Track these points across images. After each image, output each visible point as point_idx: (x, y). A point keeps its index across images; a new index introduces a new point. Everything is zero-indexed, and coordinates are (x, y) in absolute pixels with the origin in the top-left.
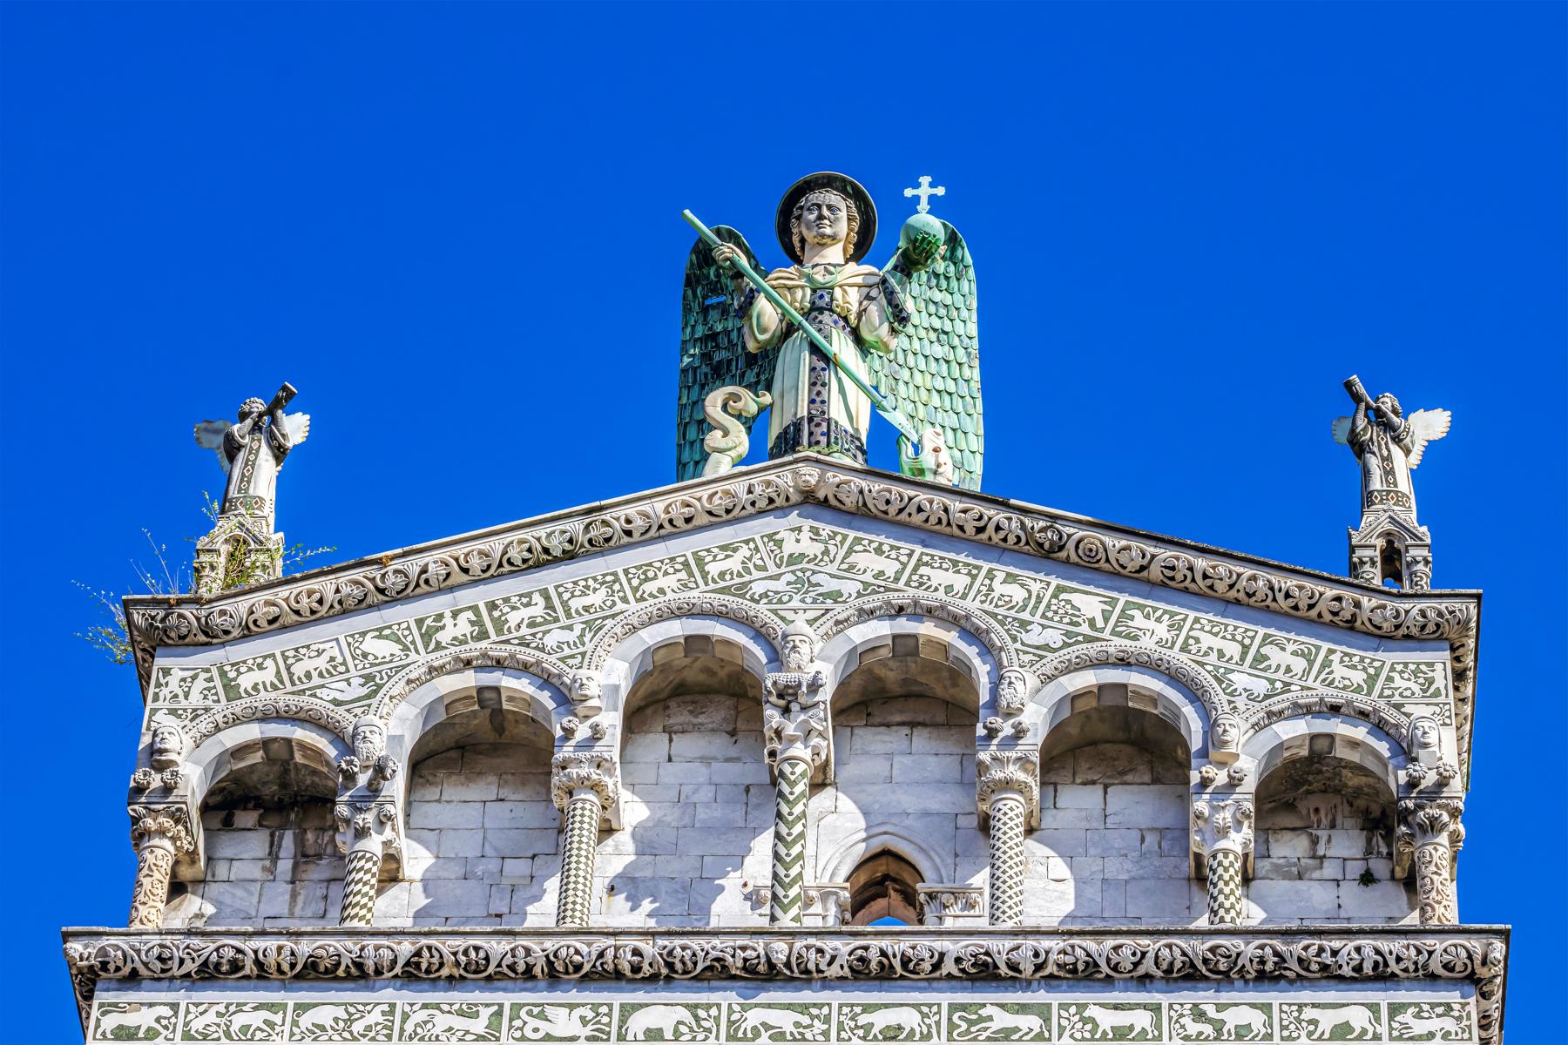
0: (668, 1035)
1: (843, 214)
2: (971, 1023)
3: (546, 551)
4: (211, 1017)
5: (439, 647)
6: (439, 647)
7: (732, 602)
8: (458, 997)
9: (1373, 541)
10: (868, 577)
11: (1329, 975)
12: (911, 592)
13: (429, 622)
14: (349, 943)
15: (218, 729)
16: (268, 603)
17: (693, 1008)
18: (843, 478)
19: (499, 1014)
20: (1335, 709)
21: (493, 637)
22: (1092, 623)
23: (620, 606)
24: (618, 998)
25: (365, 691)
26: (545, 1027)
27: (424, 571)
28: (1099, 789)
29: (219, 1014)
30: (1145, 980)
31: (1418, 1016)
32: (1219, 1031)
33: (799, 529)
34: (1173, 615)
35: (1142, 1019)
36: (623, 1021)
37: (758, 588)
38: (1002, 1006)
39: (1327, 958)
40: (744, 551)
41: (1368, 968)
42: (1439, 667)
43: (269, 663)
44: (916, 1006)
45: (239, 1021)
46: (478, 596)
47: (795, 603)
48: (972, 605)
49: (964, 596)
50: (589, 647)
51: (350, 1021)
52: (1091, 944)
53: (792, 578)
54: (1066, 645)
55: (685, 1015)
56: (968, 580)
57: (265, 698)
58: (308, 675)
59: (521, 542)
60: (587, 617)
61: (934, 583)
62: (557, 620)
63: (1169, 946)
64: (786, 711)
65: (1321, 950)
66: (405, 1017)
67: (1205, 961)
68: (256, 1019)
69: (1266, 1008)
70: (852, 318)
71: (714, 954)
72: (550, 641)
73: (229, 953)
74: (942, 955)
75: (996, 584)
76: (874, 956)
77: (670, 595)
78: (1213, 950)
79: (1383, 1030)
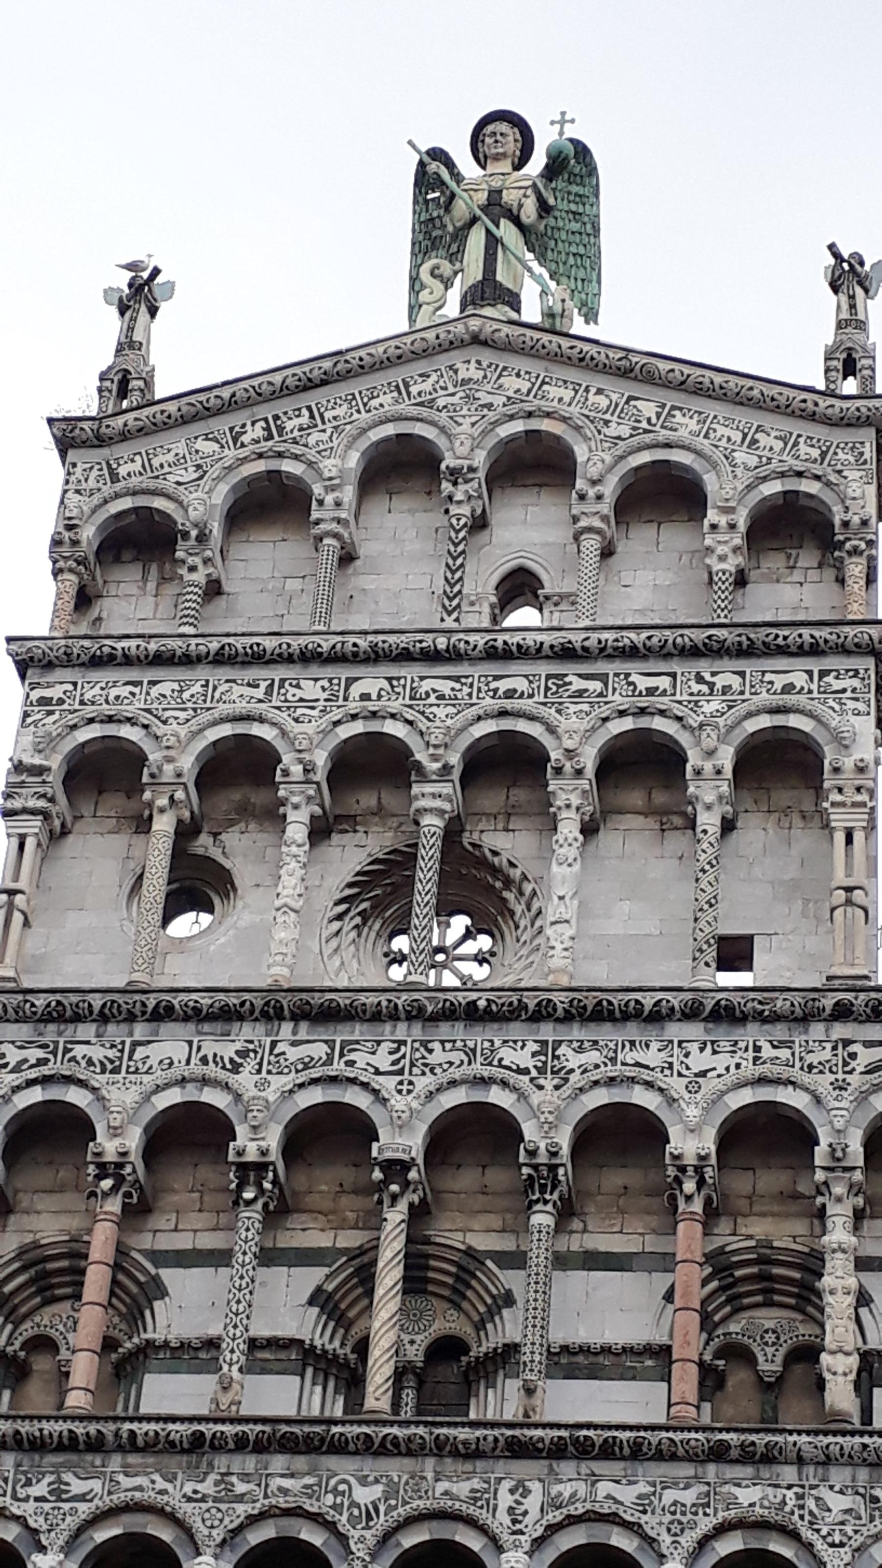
0: (374, 697)
1: (511, 138)
2: (559, 686)
3: (310, 380)
4: (97, 690)
5: (243, 445)
6: (243, 445)
7: (424, 412)
9: (837, 355)
10: (510, 393)
11: (783, 651)
12: (536, 402)
13: (237, 429)
14: (179, 642)
15: (106, 502)
16: (136, 419)
17: (389, 679)
18: (495, 327)
19: (272, 685)
20: (800, 474)
21: (277, 438)
22: (649, 420)
23: (356, 416)
24: (344, 672)
25: (196, 475)
26: (299, 694)
27: (233, 395)
28: (655, 525)
29: (102, 689)
30: (668, 656)
31: (837, 678)
32: (712, 690)
33: (469, 362)
34: (700, 413)
35: (664, 683)
36: (347, 689)
37: (441, 402)
38: (580, 676)
39: (780, 640)
40: (434, 377)
41: (806, 647)
42: (868, 445)
43: (138, 458)
44: (526, 676)
45: (113, 692)
46: (266, 411)
47: (464, 412)
48: (574, 410)
49: (570, 405)
50: (335, 443)
51: (181, 691)
52: (632, 635)
53: (462, 394)
54: (632, 436)
55: (385, 684)
56: (572, 393)
57: (135, 481)
58: (162, 466)
59: (294, 375)
60: (335, 423)
61: (551, 396)
62: (316, 426)
63: (682, 636)
64: (455, 484)
65: (777, 636)
66: (215, 688)
67: (705, 644)
68: (125, 691)
69: (742, 674)
70: (515, 212)
71: (402, 645)
72: (311, 440)
73: (106, 650)
74: (542, 644)
75: (590, 396)
76: (499, 644)
77: (387, 408)
78: (709, 637)
79: (814, 687)
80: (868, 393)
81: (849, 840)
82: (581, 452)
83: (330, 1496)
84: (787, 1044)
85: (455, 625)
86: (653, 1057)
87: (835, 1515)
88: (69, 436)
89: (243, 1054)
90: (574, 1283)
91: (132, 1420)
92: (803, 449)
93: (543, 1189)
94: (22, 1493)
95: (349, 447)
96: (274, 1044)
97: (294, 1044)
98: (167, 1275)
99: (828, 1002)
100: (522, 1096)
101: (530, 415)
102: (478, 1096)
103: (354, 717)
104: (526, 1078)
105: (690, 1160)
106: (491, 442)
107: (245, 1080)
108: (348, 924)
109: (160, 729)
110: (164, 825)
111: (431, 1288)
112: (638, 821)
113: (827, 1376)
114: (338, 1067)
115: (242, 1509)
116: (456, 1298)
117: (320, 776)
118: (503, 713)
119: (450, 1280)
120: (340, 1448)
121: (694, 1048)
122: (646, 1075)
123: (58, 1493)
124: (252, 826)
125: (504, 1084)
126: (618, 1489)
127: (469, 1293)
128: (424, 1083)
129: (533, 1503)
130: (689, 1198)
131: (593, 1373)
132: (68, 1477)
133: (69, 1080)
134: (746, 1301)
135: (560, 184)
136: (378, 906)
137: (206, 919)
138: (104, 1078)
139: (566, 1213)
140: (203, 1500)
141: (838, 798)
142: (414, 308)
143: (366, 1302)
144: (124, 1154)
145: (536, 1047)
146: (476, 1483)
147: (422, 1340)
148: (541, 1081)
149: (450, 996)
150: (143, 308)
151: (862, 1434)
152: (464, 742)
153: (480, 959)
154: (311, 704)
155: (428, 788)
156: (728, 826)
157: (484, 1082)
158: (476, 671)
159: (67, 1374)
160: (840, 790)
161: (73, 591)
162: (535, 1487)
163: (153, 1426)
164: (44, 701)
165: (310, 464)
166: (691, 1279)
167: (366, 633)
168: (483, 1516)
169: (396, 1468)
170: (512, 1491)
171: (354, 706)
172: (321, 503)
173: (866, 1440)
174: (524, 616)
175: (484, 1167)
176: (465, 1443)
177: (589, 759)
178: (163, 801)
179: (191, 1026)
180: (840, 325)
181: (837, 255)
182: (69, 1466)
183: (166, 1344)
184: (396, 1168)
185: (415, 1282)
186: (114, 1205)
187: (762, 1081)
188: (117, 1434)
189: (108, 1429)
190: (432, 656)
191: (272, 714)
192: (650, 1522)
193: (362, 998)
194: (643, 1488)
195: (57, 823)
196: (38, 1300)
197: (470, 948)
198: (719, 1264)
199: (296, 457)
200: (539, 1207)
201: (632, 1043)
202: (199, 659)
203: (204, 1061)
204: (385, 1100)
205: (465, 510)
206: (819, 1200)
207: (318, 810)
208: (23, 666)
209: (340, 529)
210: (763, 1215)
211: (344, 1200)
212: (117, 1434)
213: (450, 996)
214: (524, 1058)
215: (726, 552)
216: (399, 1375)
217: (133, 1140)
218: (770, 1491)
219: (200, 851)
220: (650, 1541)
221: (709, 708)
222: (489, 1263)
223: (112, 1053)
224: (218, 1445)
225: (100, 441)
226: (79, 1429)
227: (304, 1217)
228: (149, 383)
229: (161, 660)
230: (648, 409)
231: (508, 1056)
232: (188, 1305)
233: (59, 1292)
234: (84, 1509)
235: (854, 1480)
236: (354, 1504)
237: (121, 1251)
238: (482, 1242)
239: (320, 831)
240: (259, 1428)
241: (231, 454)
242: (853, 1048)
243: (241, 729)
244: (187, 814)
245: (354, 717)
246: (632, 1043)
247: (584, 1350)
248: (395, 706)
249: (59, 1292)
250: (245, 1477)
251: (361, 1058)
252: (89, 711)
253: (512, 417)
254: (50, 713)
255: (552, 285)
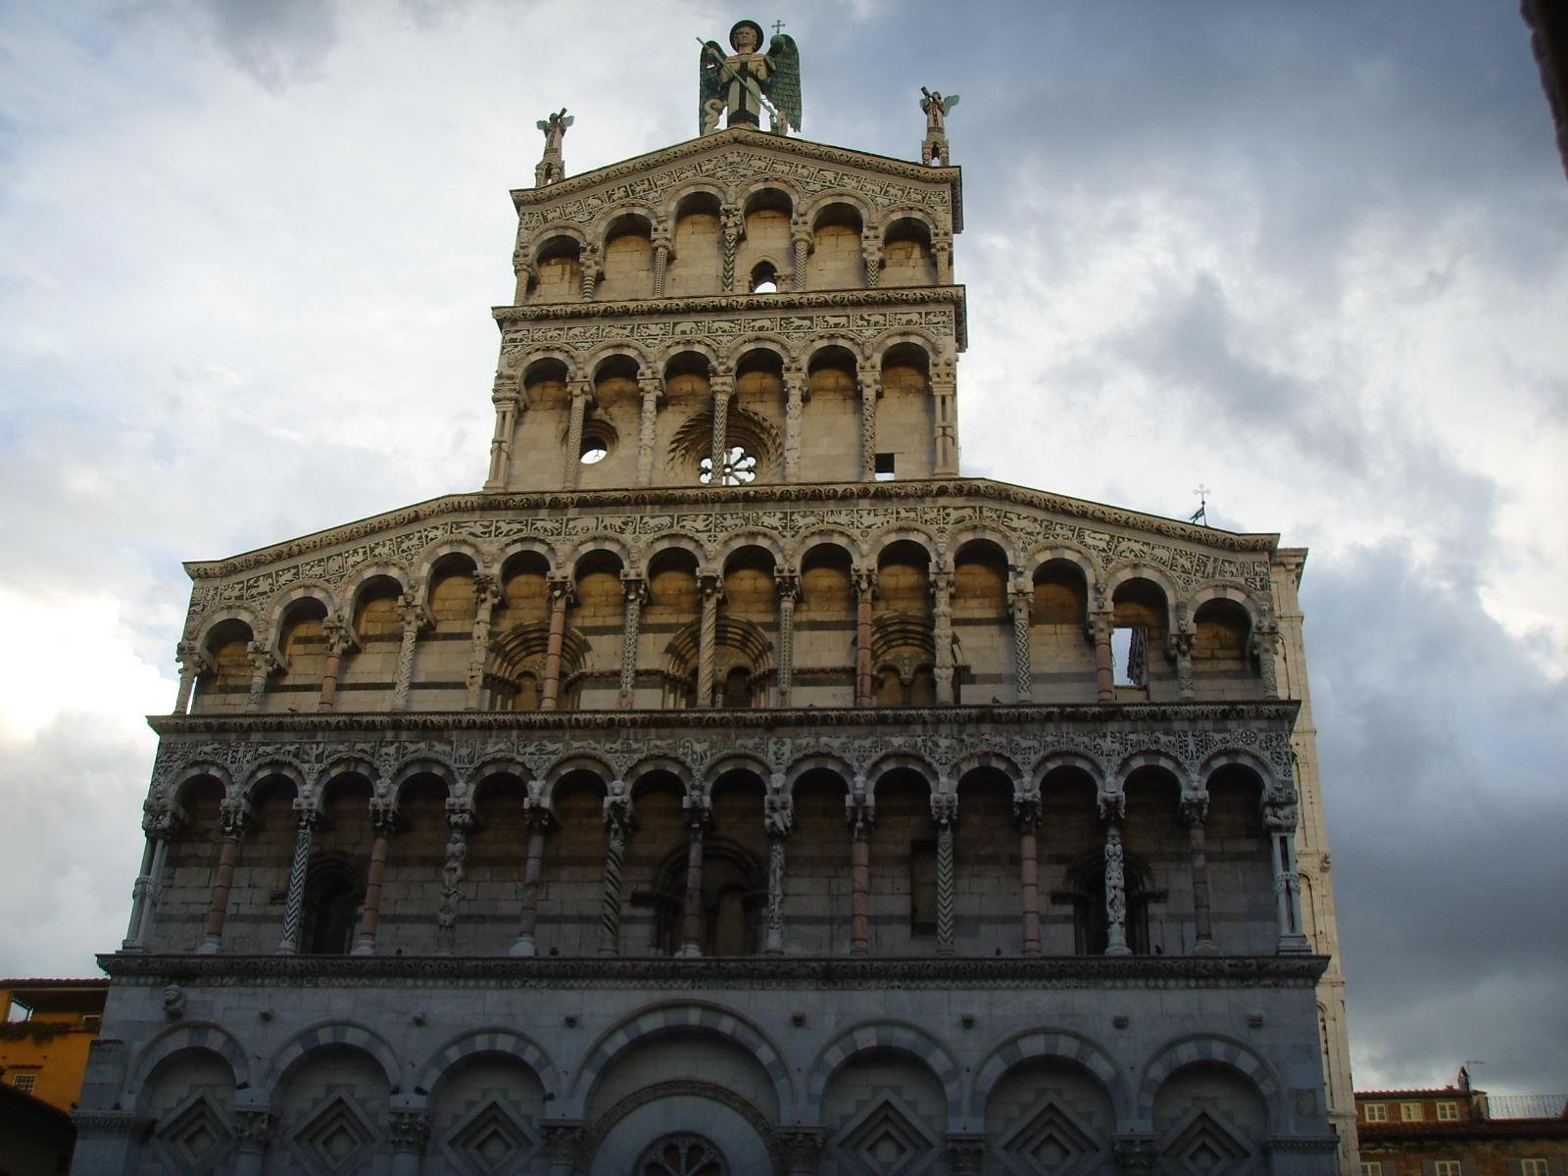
1: (751, 36)
4: (540, 334)
8: (620, 324)
11: (906, 302)
24: (672, 320)
26: (648, 332)
30: (846, 305)
35: (843, 321)
37: (719, 175)
45: (550, 334)
46: (626, 182)
48: (790, 177)
55: (694, 325)
64: (728, 217)
68: (555, 333)
69: (885, 315)
72: (650, 197)
80: (944, 165)
81: (943, 402)
82: (795, 199)
83: (681, 750)
84: (914, 510)
85: (730, 293)
86: (843, 519)
87: (942, 749)
88: (522, 200)
89: (626, 523)
90: (804, 637)
91: (577, 713)
92: (913, 195)
93: (787, 589)
94: (522, 751)
95: (670, 200)
96: (642, 518)
97: (652, 517)
98: (592, 640)
99: (935, 487)
100: (775, 542)
101: (767, 179)
102: (751, 542)
103: (678, 343)
104: (776, 532)
105: (864, 572)
106: (747, 195)
107: (627, 537)
108: (678, 454)
109: (574, 353)
110: (579, 404)
111: (729, 642)
112: (831, 396)
113: (938, 680)
114: (676, 529)
115: (637, 756)
116: (743, 645)
117: (661, 375)
118: (758, 339)
119: (739, 638)
120: (684, 724)
121: (865, 513)
122: (840, 528)
123: (541, 750)
124: (625, 403)
125: (765, 535)
126: (831, 741)
127: (750, 644)
128: (722, 536)
129: (787, 749)
130: (863, 591)
131: (816, 683)
132: (545, 742)
133: (535, 540)
134: (894, 643)
135: (779, 58)
136: (694, 443)
137: (602, 453)
138: (555, 537)
139: (799, 600)
140: (615, 752)
141: (938, 379)
142: (703, 125)
143: (694, 650)
144: (566, 578)
145: (781, 516)
146: (757, 740)
147: (725, 669)
148: (785, 533)
149: (735, 490)
150: (558, 130)
151: (955, 708)
152: (737, 355)
153: (749, 470)
154: (654, 337)
155: (719, 380)
156: (879, 395)
157: (754, 535)
158: (744, 317)
159: (542, 691)
160: (938, 376)
161: (525, 282)
162: (788, 741)
163: (588, 716)
164: (512, 340)
165: (650, 209)
166: (866, 632)
167: (682, 298)
168: (762, 756)
169: (715, 735)
170: (776, 743)
171: (678, 338)
172: (656, 230)
173: (958, 711)
174: (767, 287)
175: (755, 579)
176: (751, 720)
177: (804, 361)
178: (577, 391)
179: (597, 509)
180: (930, 130)
181: (926, 94)
182: (544, 737)
183: (592, 675)
184: (709, 581)
185: (721, 639)
186: (561, 604)
187: (900, 530)
188: (569, 720)
189: (565, 718)
190: (719, 310)
191: (635, 344)
192: (848, 757)
193: (688, 492)
194: (843, 739)
195: (522, 404)
196: (524, 654)
197: (743, 464)
198: (880, 625)
199: (642, 206)
200: (785, 598)
201: (832, 512)
202: (594, 315)
203: (605, 527)
204: (702, 546)
205: (734, 231)
206: (932, 590)
207: (660, 393)
208: (500, 323)
209: (667, 243)
210: (903, 599)
211: (684, 599)
212: (569, 720)
213: (735, 490)
214: (775, 522)
215: (873, 250)
216: (714, 690)
217: (569, 570)
218: (909, 739)
219: (598, 417)
220: (848, 766)
221: (867, 333)
222: (760, 629)
223: (557, 525)
224: (622, 724)
225: (537, 201)
226: (550, 718)
227: (662, 607)
228: (562, 169)
229: (575, 316)
230: (830, 176)
231: (767, 520)
232: (603, 653)
233: (534, 649)
234: (554, 758)
235: (952, 731)
236: (694, 753)
237: (566, 626)
238: (756, 618)
239: (662, 404)
240: (643, 715)
241: (607, 206)
242: (947, 511)
243: (618, 352)
244: (590, 398)
245: (678, 343)
246: (832, 512)
247: (812, 671)
248: (699, 337)
249: (534, 649)
250: (636, 741)
251: (688, 524)
252: (537, 345)
253: (757, 181)
254: (516, 346)
255: (776, 111)
